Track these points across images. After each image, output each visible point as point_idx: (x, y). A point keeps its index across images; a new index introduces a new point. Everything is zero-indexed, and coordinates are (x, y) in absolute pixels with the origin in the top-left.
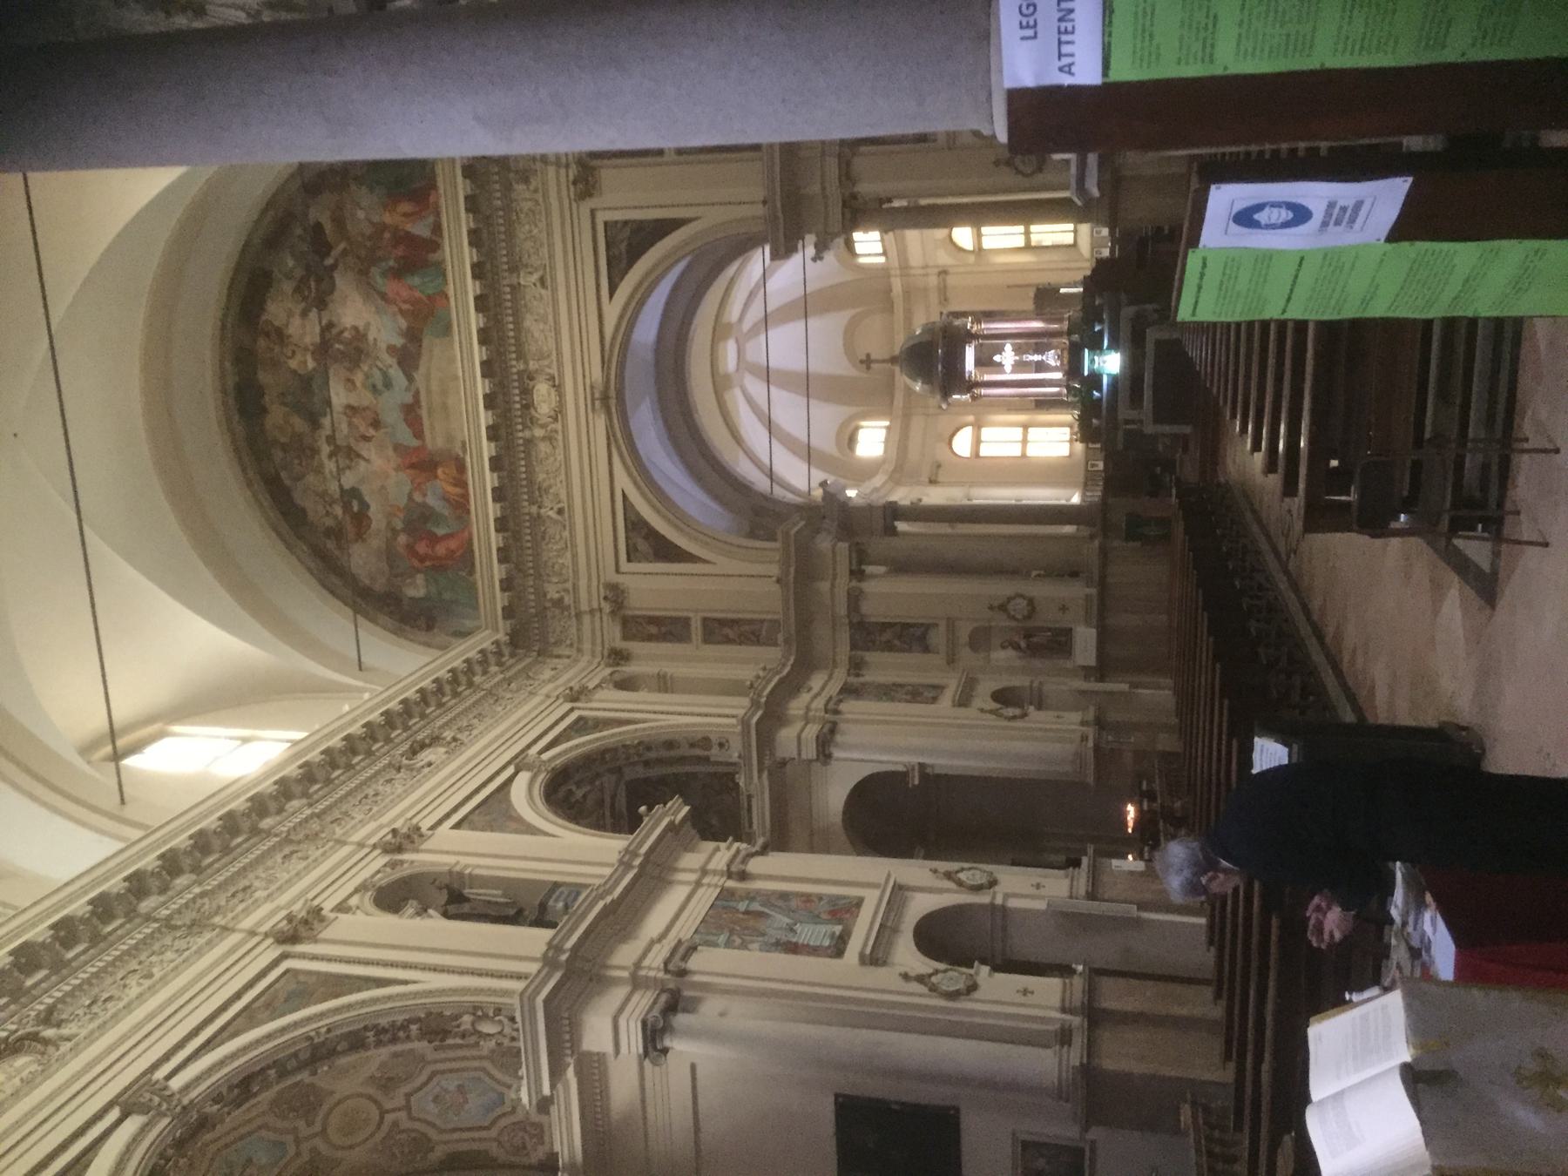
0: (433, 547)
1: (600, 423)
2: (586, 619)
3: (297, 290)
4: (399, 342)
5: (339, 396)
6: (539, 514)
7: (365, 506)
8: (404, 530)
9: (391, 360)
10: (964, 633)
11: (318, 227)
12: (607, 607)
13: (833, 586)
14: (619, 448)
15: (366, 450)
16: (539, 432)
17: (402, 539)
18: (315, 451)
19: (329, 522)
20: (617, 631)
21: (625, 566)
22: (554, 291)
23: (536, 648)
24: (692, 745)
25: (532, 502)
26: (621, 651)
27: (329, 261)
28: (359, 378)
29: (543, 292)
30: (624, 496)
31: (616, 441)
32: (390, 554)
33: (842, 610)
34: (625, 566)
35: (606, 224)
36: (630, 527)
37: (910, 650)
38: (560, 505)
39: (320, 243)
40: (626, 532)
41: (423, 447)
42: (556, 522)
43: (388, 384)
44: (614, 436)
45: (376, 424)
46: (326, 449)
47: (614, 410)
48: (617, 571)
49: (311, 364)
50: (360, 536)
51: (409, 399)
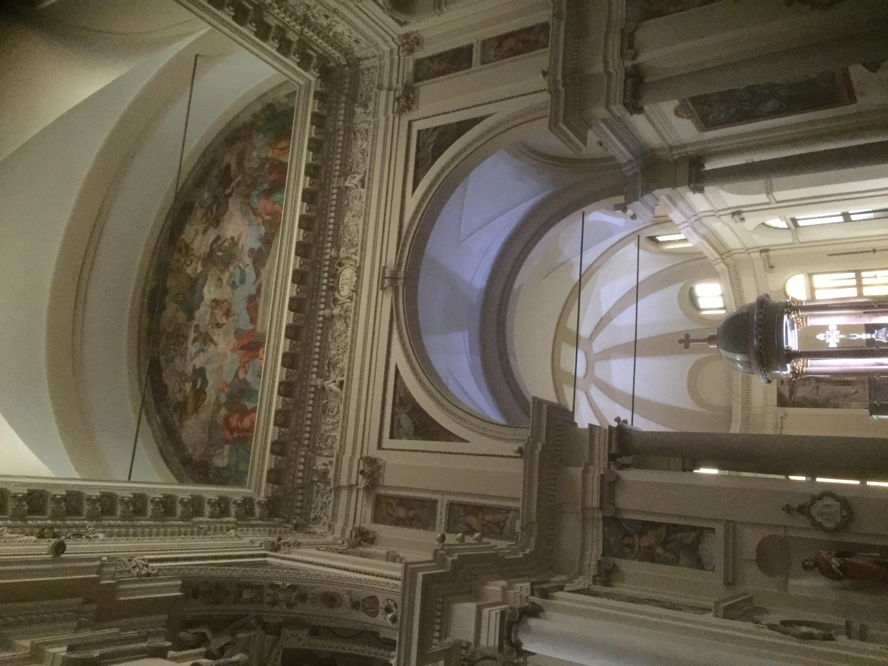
0: (242, 421)
1: (387, 301)
2: (344, 494)
3: (205, 215)
4: (257, 245)
5: (210, 292)
6: (323, 388)
7: (205, 381)
8: (225, 404)
9: (248, 260)
10: (751, 540)
11: (228, 167)
12: (362, 482)
13: (585, 472)
14: (399, 326)
15: (218, 336)
16: (336, 311)
17: (223, 412)
18: (186, 338)
19: (179, 397)
20: (368, 512)
21: (387, 442)
22: (370, 188)
23: (294, 522)
24: (356, 605)
25: (320, 375)
26: (368, 532)
27: (228, 191)
28: (226, 277)
29: (362, 190)
30: (397, 371)
31: (398, 319)
32: (211, 427)
33: (594, 501)
34: (387, 442)
35: (419, 132)
36: (398, 401)
37: (675, 562)
38: (341, 379)
39: (226, 179)
40: (393, 408)
41: (253, 331)
42: (336, 395)
43: (242, 281)
44: (398, 313)
45: (228, 313)
46: (192, 335)
47: (401, 288)
48: (380, 447)
49: (200, 269)
50: (196, 409)
51: (254, 292)
